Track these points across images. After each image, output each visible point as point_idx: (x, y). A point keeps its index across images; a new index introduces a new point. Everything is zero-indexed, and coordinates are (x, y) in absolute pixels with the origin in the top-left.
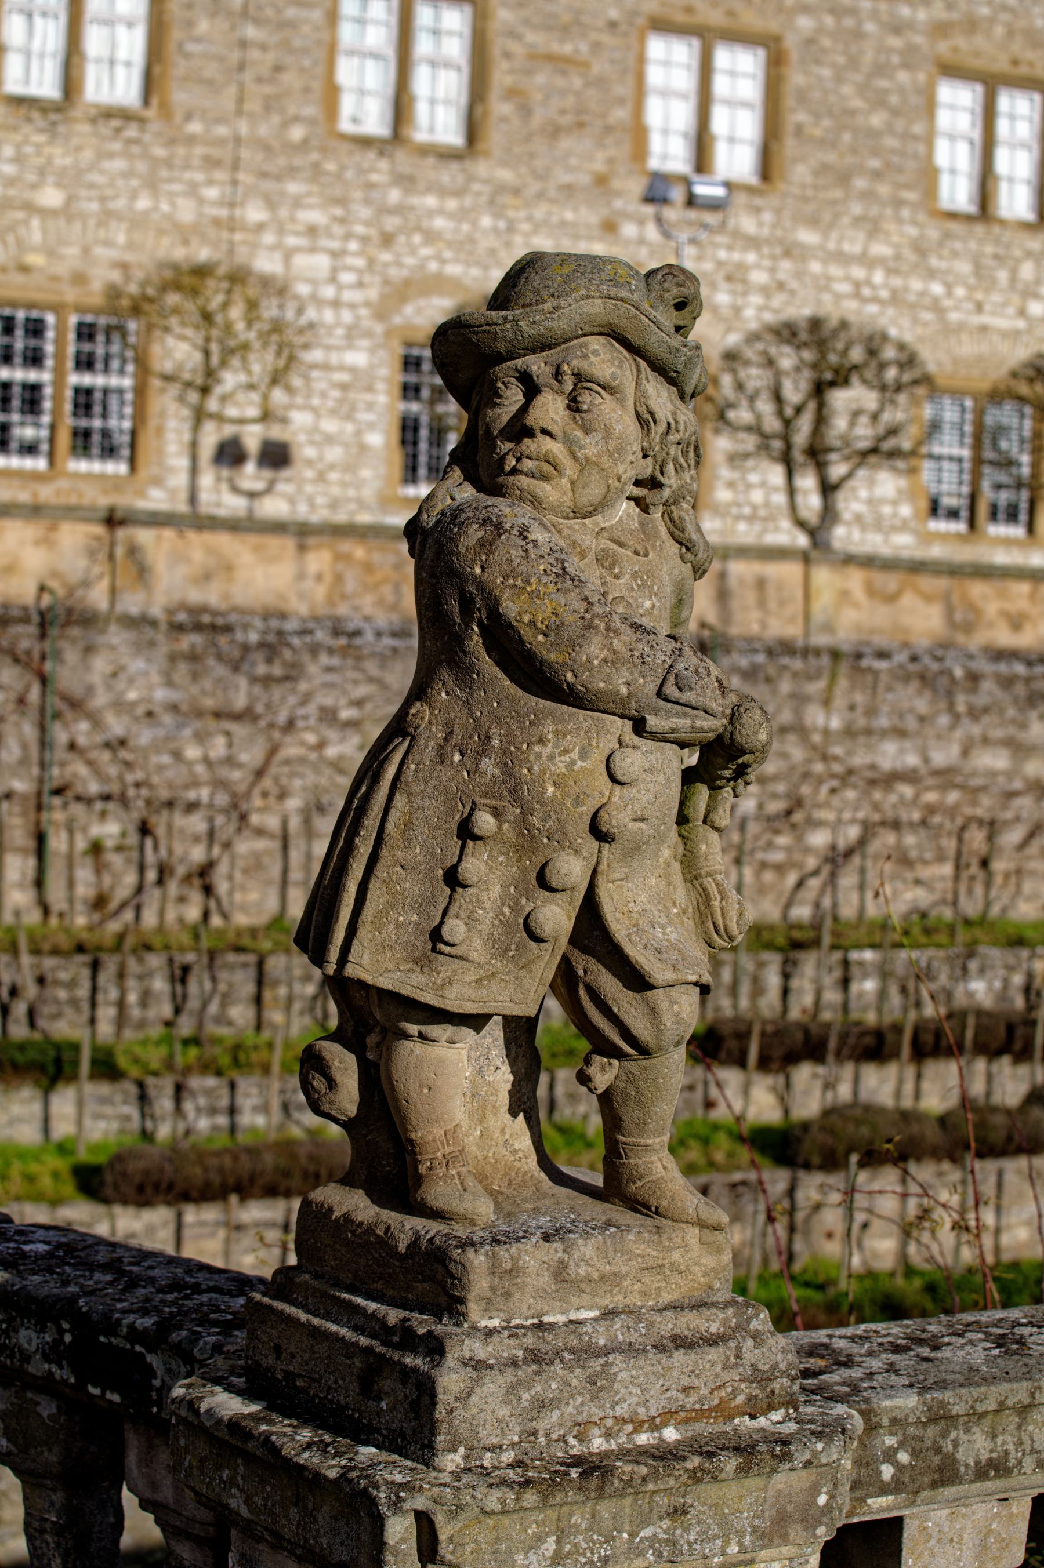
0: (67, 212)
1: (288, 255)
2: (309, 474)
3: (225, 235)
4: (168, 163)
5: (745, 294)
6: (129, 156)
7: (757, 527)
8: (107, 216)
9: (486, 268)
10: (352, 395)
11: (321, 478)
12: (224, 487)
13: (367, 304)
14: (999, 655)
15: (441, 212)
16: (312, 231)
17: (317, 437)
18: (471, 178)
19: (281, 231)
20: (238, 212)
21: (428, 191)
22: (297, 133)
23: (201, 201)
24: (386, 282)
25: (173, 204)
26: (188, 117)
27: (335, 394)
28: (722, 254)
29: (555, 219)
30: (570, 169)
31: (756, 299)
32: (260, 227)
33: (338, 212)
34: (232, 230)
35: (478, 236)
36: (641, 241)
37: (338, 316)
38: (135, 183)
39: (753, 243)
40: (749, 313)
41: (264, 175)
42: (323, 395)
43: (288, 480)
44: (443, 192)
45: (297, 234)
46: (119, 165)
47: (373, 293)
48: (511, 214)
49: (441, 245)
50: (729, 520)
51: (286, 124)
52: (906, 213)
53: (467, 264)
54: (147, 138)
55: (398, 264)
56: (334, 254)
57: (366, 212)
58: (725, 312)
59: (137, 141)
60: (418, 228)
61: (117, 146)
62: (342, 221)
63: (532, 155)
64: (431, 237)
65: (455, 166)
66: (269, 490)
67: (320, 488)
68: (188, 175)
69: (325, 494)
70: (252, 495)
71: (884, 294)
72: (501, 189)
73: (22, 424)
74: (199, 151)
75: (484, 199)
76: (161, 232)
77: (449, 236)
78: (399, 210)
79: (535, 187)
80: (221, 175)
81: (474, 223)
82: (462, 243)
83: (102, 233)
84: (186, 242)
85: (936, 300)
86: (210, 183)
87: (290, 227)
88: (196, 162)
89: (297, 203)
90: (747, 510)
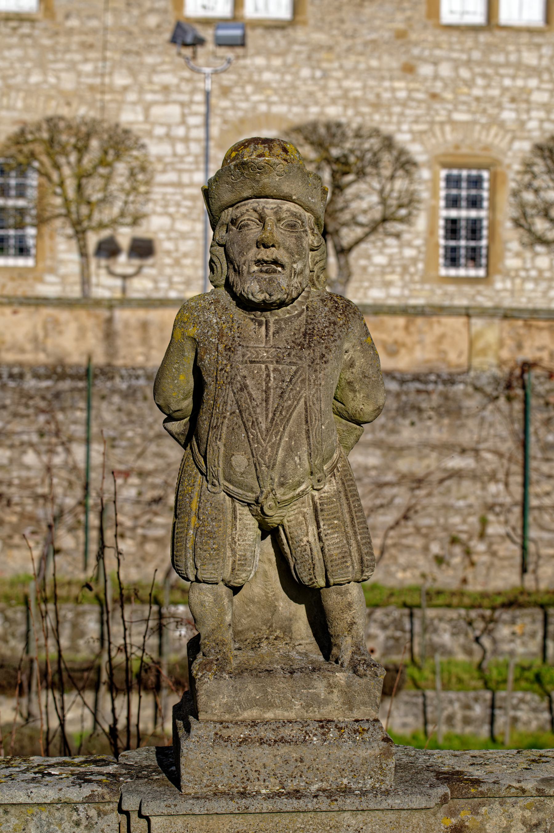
1: (147, 108)
2: (168, 261)
3: (98, 96)
4: (54, 50)
5: (528, 111)
6: (24, 47)
7: (543, 285)
9: (306, 106)
11: (177, 263)
12: (103, 272)
15: (268, 68)
16: (166, 89)
17: (173, 235)
18: (292, 42)
19: (141, 91)
20: (107, 80)
21: (258, 53)
23: (79, 74)
24: (225, 122)
25: (58, 78)
26: (67, 16)
27: (188, 203)
28: (507, 82)
29: (362, 66)
30: (373, 29)
32: (125, 89)
34: (103, 92)
35: (298, 83)
36: (436, 77)
37: (188, 148)
38: (29, 65)
40: (532, 125)
41: (127, 52)
42: (178, 205)
43: (152, 266)
44: (269, 54)
45: (154, 92)
46: (17, 53)
48: (325, 65)
49: (269, 92)
50: (518, 281)
51: (143, 15)
53: (290, 104)
54: (37, 32)
55: (234, 108)
56: (182, 104)
58: (510, 125)
59: (29, 36)
60: (250, 81)
61: (15, 40)
62: (188, 80)
63: (342, 21)
64: (260, 87)
65: (278, 34)
66: (137, 273)
67: (177, 270)
68: (68, 57)
69: (181, 275)
70: (125, 277)
72: (319, 48)
74: (76, 39)
75: (303, 56)
76: (49, 98)
77: (274, 85)
79: (345, 44)
81: (296, 75)
82: (285, 89)
84: (68, 104)
86: (86, 60)
87: (148, 87)
88: (74, 47)
89: (154, 70)
90: (533, 273)
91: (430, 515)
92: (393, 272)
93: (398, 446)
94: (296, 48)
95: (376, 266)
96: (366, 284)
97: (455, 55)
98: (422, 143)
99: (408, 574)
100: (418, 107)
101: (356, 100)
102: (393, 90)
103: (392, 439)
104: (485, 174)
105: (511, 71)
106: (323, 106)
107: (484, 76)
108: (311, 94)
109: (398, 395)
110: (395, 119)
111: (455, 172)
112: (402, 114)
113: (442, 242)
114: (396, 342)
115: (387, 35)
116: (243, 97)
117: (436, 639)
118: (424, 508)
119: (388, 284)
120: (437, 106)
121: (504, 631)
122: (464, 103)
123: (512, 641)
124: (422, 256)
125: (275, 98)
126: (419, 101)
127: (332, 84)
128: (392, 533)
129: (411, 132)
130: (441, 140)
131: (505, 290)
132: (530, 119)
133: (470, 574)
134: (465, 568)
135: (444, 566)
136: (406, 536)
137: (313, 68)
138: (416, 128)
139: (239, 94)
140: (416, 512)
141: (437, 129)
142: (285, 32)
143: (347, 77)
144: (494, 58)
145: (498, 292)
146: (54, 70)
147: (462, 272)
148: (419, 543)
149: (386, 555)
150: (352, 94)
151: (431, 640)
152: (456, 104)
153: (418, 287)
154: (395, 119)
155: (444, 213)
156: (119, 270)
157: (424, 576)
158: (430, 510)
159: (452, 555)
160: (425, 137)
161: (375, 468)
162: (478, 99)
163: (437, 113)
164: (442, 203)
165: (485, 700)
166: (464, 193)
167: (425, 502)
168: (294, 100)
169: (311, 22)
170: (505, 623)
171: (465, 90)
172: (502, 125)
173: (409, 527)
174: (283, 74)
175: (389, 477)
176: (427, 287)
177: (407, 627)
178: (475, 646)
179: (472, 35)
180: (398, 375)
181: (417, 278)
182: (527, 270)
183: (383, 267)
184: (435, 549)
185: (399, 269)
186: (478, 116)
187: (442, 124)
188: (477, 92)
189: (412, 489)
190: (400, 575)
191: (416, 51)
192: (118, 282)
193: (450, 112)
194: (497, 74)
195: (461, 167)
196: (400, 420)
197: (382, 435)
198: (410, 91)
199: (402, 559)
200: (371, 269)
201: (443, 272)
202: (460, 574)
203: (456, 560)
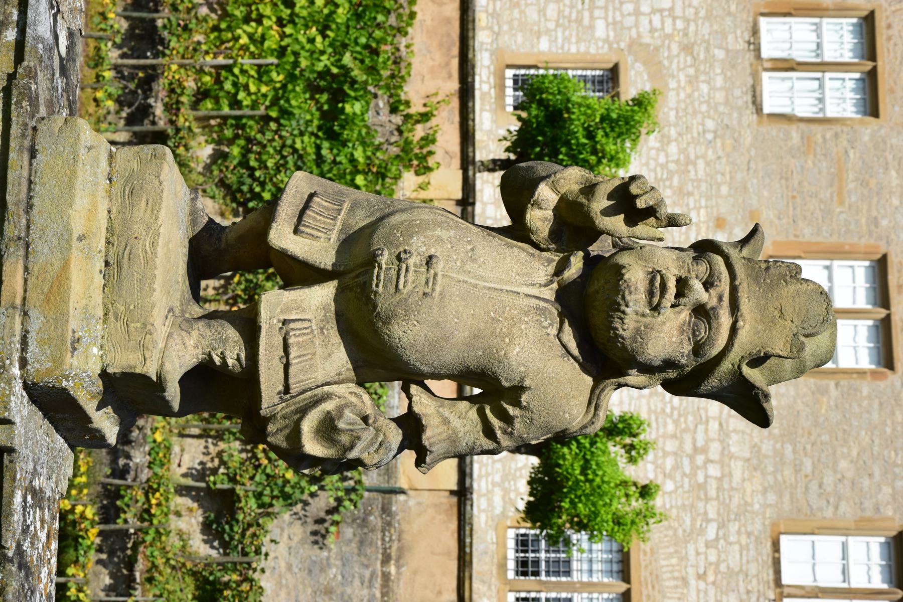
10: (574, 25)
13: (639, 35)
21: (726, 79)
24: (657, 49)
27: (574, 16)
33: (702, 13)
35: (699, 117)
47: (647, 39)
52: (771, 498)
71: (701, 478)
75: (726, 121)
85: (702, 531)
94: (735, 115)
102: (698, 209)
108: (688, 129)
115: (755, 202)
116: (682, 66)
127: (701, 150)
137: (715, 132)
139: (686, 61)
142: (750, 105)
143: (708, 164)
169: (763, 129)
174: (708, 102)
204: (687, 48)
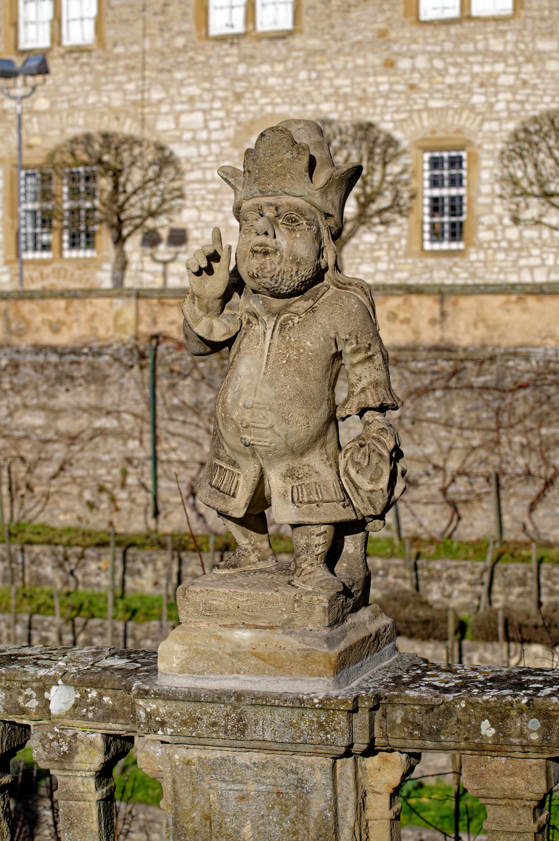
0: (51, 112)
1: (177, 116)
3: (139, 110)
4: (105, 74)
5: (496, 94)
6: (82, 73)
7: (513, 255)
8: (73, 109)
9: (304, 105)
10: (220, 196)
12: (147, 259)
13: (228, 139)
14: (39, 349)
15: (272, 74)
16: (191, 99)
17: (200, 225)
18: (292, 49)
19: (173, 103)
20: (146, 96)
21: (264, 62)
22: (180, 42)
23: (125, 92)
24: (239, 124)
25: (109, 97)
26: (115, 45)
27: (211, 197)
28: (477, 69)
29: (350, 65)
30: (358, 31)
31: (505, 96)
32: (160, 102)
33: (207, 85)
34: (143, 107)
35: (297, 85)
36: (413, 69)
37: (210, 149)
38: (87, 88)
39: (501, 57)
41: (161, 71)
42: (203, 199)
43: (186, 252)
44: (272, 61)
45: (182, 103)
46: (78, 79)
47: (231, 133)
48: (319, 67)
49: (274, 95)
50: (490, 252)
51: (173, 38)
53: (291, 104)
54: (93, 61)
55: (246, 111)
56: (204, 111)
57: (223, 83)
58: (481, 109)
59: (87, 64)
60: (258, 87)
61: (76, 69)
62: (209, 90)
63: (332, 27)
64: (266, 91)
65: (280, 43)
66: (173, 260)
68: (117, 78)
70: (165, 263)
73: (42, 233)
74: (122, 63)
75: (300, 61)
76: (102, 115)
77: (278, 88)
78: (245, 78)
79: (335, 46)
80: (136, 75)
81: (295, 78)
82: (286, 91)
83: (71, 120)
84: (117, 118)
86: (130, 80)
87: (177, 99)
88: (120, 70)
89: (182, 84)
90: (504, 244)
91: (82, 468)
92: (380, 249)
93: (57, 409)
94: (295, 54)
95: (366, 243)
96: (358, 261)
97: (429, 48)
98: (403, 130)
99: (68, 517)
100: (399, 98)
101: (346, 95)
102: (377, 84)
103: (53, 403)
104: (464, 155)
105: (479, 58)
106: (318, 104)
107: (455, 64)
108: (308, 94)
109: (56, 366)
110: (378, 110)
111: (437, 154)
112: (385, 106)
113: (427, 219)
114: (59, 322)
115: (370, 35)
116: (252, 101)
117: (41, 571)
118: (78, 461)
119: (376, 260)
120: (415, 96)
121: (93, 566)
122: (439, 91)
123: (98, 575)
124: (405, 233)
125: (278, 100)
126: (400, 93)
127: (326, 83)
128: (54, 482)
129: (393, 121)
130: (419, 126)
131: (479, 261)
132: (498, 101)
133: (115, 518)
134: (112, 513)
135: (95, 511)
136: (65, 484)
137: (309, 71)
138: (397, 117)
139: (249, 99)
140: (71, 464)
141: (415, 116)
142: (286, 41)
143: (337, 76)
144: (463, 48)
145: (472, 262)
146: (107, 91)
147: (445, 246)
148: (75, 490)
149: (51, 500)
150: (341, 92)
151: (37, 571)
152: (432, 92)
153: (402, 261)
154: (378, 110)
155: (428, 192)
156: (159, 257)
157: (79, 519)
158: (83, 463)
159: (101, 502)
160: (405, 125)
161: (40, 427)
162: (450, 87)
163: (416, 103)
164: (427, 184)
165: (24, 622)
166: (446, 173)
167: (78, 456)
168: (294, 100)
169: (307, 30)
170: (92, 559)
171: (439, 79)
172: (473, 109)
173: (66, 477)
174: (284, 78)
175: (50, 435)
176: (410, 261)
177: (20, 560)
178: (71, 579)
179: (444, 28)
180: (60, 350)
181: (401, 253)
182: (498, 242)
183: (372, 244)
184: (87, 495)
185: (385, 246)
186: (451, 102)
187: (420, 111)
188: (450, 80)
189: (69, 445)
190: (62, 517)
191: (396, 48)
192: (159, 268)
193: (426, 100)
194: (467, 62)
195: (441, 149)
196: (58, 387)
197: (44, 399)
198: (391, 84)
199: (63, 504)
200: (362, 247)
201: (428, 246)
202: (108, 518)
203: (104, 506)
204: (238, 97)
